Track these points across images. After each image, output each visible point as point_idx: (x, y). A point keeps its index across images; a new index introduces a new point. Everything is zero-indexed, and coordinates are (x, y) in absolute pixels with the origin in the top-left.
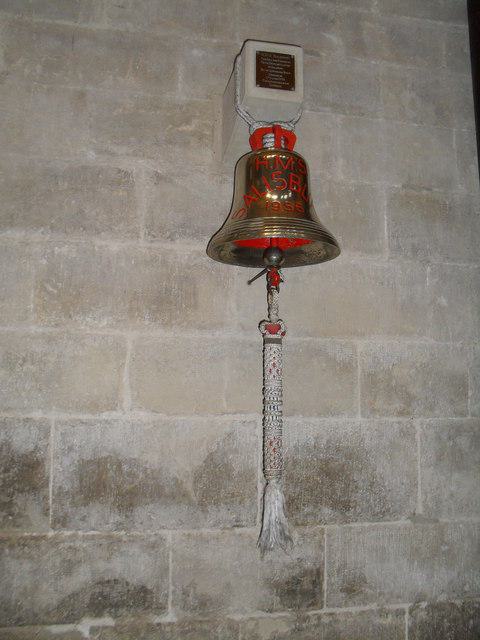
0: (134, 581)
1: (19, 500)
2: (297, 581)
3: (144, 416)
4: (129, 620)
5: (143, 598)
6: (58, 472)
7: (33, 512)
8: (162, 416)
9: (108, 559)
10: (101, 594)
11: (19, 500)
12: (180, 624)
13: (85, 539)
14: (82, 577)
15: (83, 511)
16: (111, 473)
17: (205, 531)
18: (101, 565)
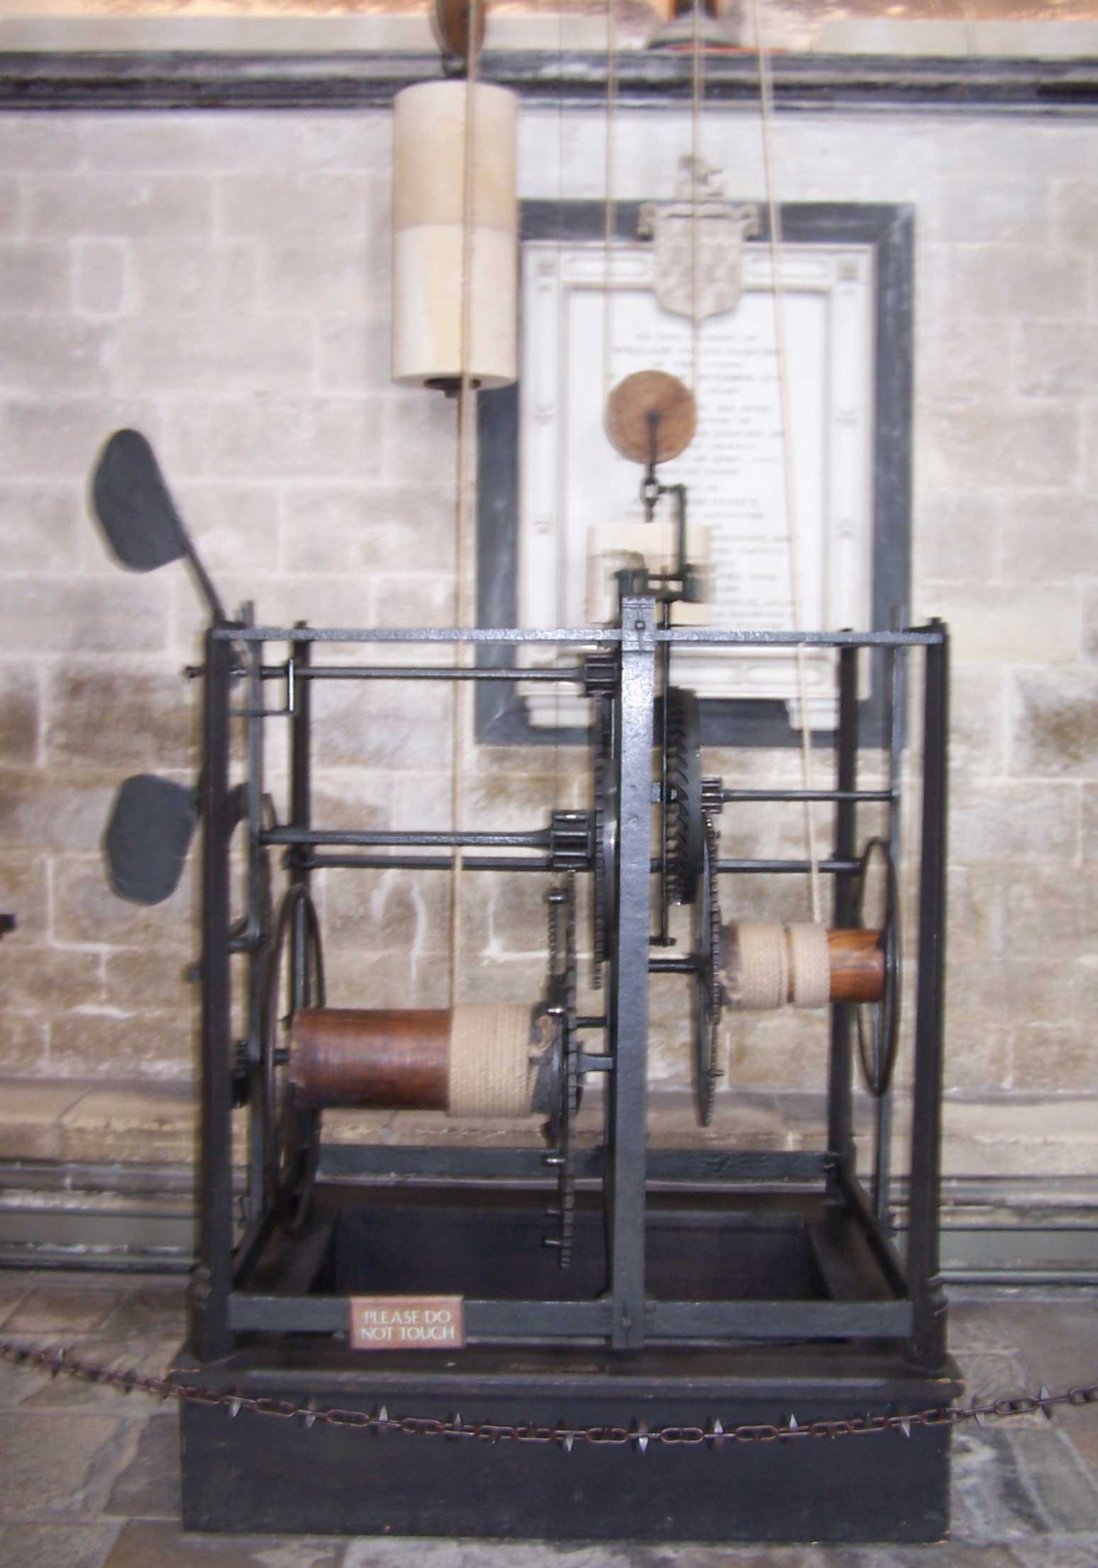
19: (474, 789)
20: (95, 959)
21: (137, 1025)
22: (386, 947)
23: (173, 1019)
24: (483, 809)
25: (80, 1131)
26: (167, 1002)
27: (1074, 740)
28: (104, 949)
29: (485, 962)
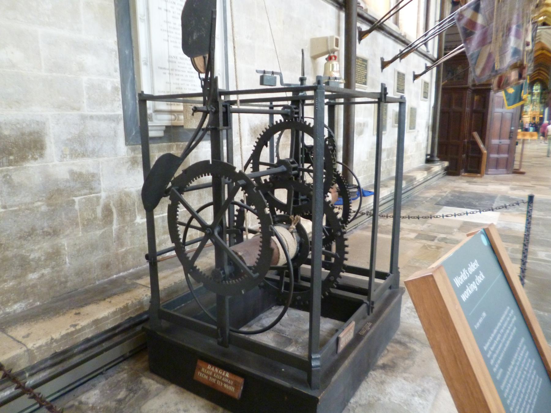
19: (127, 162)
22: (104, 227)
23: (20, 283)
24: (130, 169)
25: (40, 348)
26: (15, 277)
29: (136, 225)
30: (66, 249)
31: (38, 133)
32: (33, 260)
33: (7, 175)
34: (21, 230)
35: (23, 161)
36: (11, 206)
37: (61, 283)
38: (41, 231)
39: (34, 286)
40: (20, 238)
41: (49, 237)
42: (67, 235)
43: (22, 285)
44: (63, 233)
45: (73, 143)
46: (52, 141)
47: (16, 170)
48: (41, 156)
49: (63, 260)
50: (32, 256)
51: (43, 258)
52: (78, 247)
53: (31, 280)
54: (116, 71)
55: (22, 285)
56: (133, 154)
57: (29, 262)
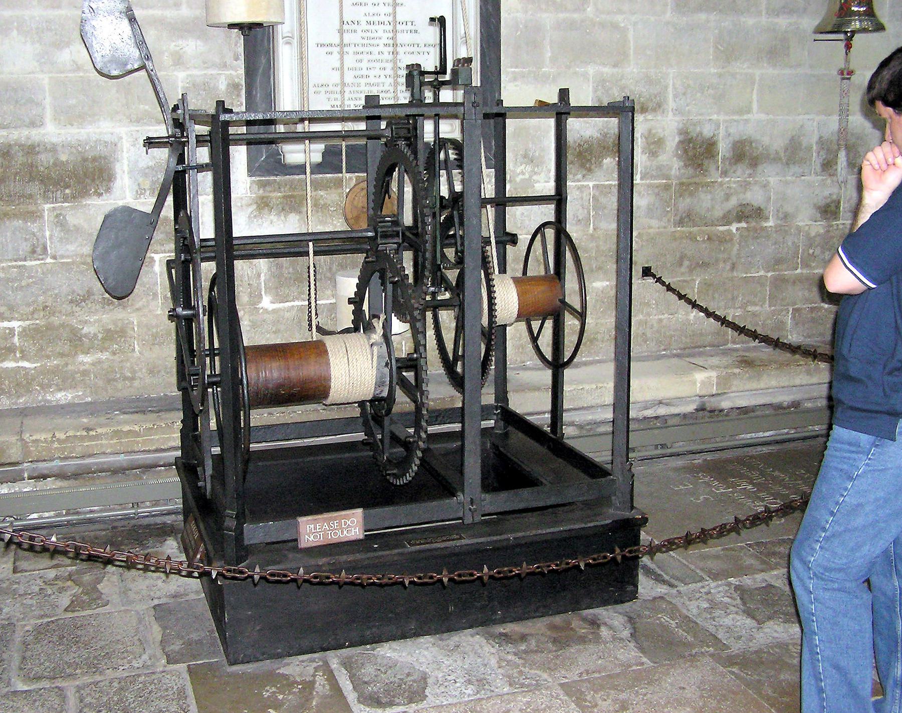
0: (756, 204)
1: (706, 162)
2: (828, 206)
3: (763, 116)
4: (753, 224)
5: (758, 213)
6: (723, 148)
7: (712, 168)
8: (771, 116)
9: (744, 193)
10: (741, 211)
11: (706, 162)
12: (776, 226)
13: (735, 182)
14: (733, 202)
15: (734, 167)
16: (747, 148)
17: (789, 178)
18: (741, 196)
19: (249, 205)
20: (12, 330)
21: (42, 371)
23: (67, 364)
26: (62, 355)
27: (589, 160)
28: (15, 324)
29: (261, 311)
30: (136, 329)
31: (105, 158)
32: (86, 336)
33: (60, 214)
34: (73, 292)
35: (83, 197)
36: (62, 257)
37: (125, 378)
38: (101, 297)
39: (85, 373)
40: (71, 302)
41: (111, 307)
42: (138, 309)
43: (70, 367)
44: (132, 305)
45: (157, 172)
46: (126, 168)
47: (72, 208)
48: (108, 190)
49: (130, 345)
50: (86, 330)
51: (100, 336)
52: (154, 330)
53: (82, 363)
54: (237, 59)
55: (70, 367)
56: (261, 191)
57: (80, 338)
